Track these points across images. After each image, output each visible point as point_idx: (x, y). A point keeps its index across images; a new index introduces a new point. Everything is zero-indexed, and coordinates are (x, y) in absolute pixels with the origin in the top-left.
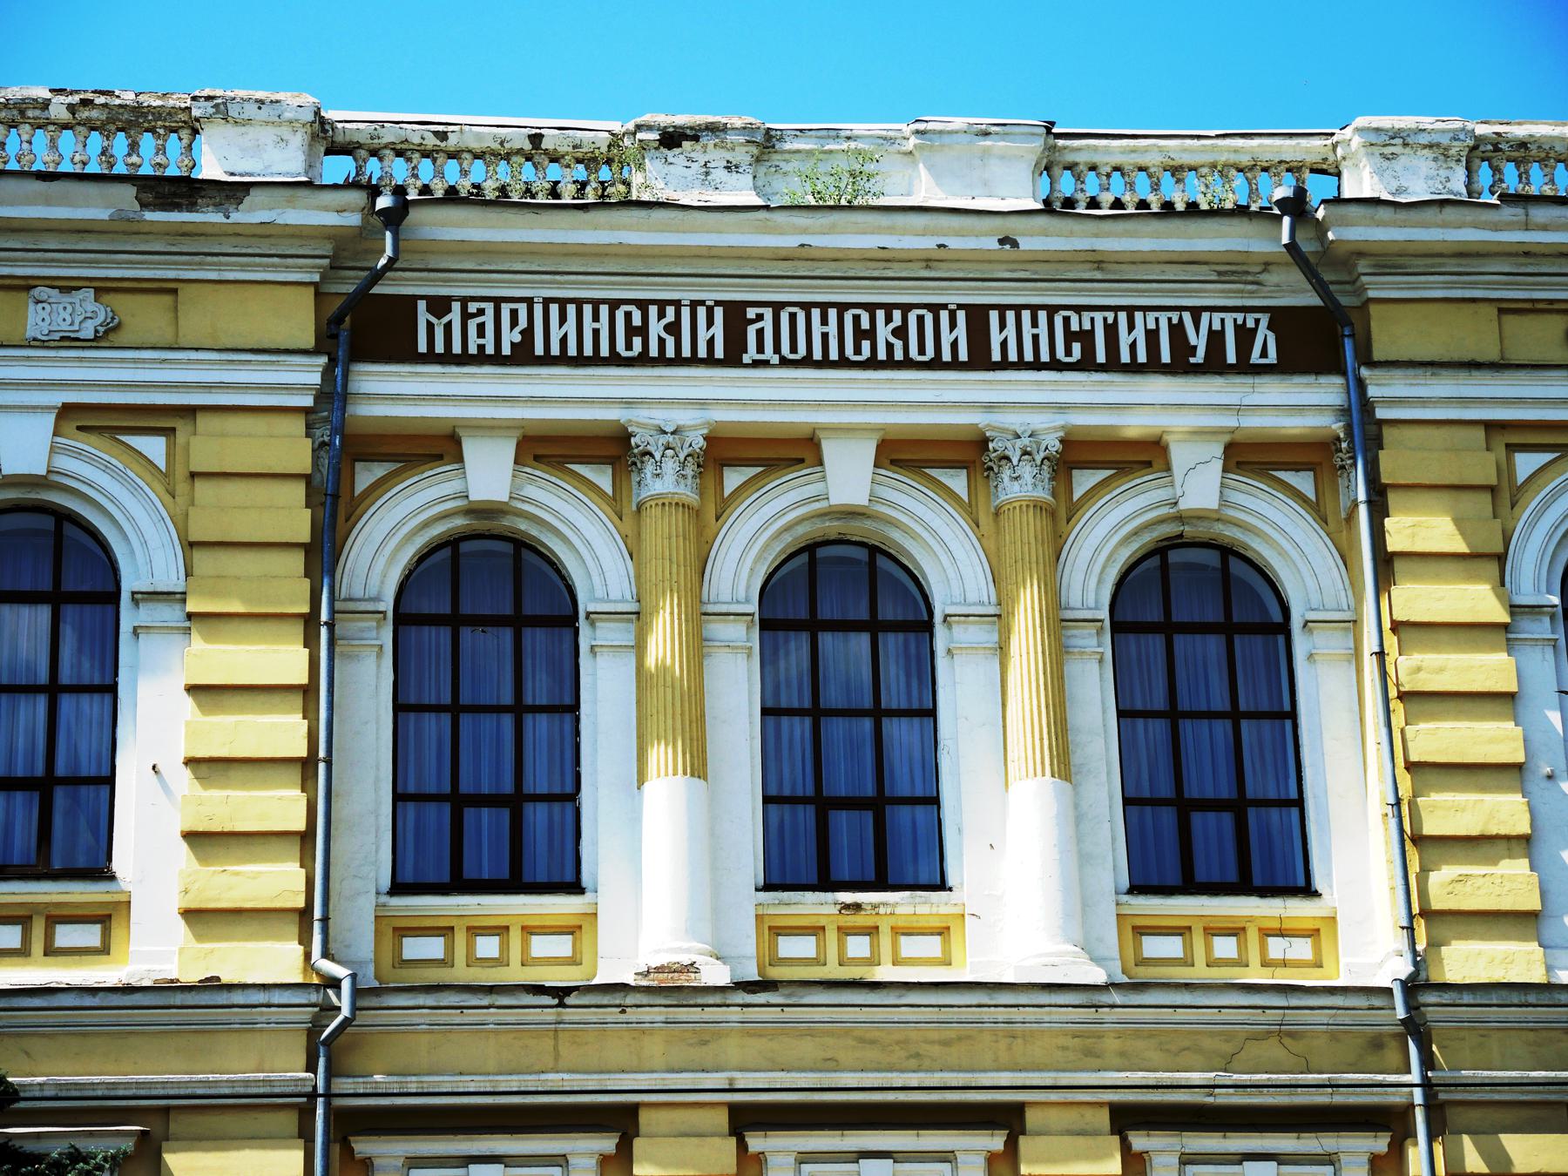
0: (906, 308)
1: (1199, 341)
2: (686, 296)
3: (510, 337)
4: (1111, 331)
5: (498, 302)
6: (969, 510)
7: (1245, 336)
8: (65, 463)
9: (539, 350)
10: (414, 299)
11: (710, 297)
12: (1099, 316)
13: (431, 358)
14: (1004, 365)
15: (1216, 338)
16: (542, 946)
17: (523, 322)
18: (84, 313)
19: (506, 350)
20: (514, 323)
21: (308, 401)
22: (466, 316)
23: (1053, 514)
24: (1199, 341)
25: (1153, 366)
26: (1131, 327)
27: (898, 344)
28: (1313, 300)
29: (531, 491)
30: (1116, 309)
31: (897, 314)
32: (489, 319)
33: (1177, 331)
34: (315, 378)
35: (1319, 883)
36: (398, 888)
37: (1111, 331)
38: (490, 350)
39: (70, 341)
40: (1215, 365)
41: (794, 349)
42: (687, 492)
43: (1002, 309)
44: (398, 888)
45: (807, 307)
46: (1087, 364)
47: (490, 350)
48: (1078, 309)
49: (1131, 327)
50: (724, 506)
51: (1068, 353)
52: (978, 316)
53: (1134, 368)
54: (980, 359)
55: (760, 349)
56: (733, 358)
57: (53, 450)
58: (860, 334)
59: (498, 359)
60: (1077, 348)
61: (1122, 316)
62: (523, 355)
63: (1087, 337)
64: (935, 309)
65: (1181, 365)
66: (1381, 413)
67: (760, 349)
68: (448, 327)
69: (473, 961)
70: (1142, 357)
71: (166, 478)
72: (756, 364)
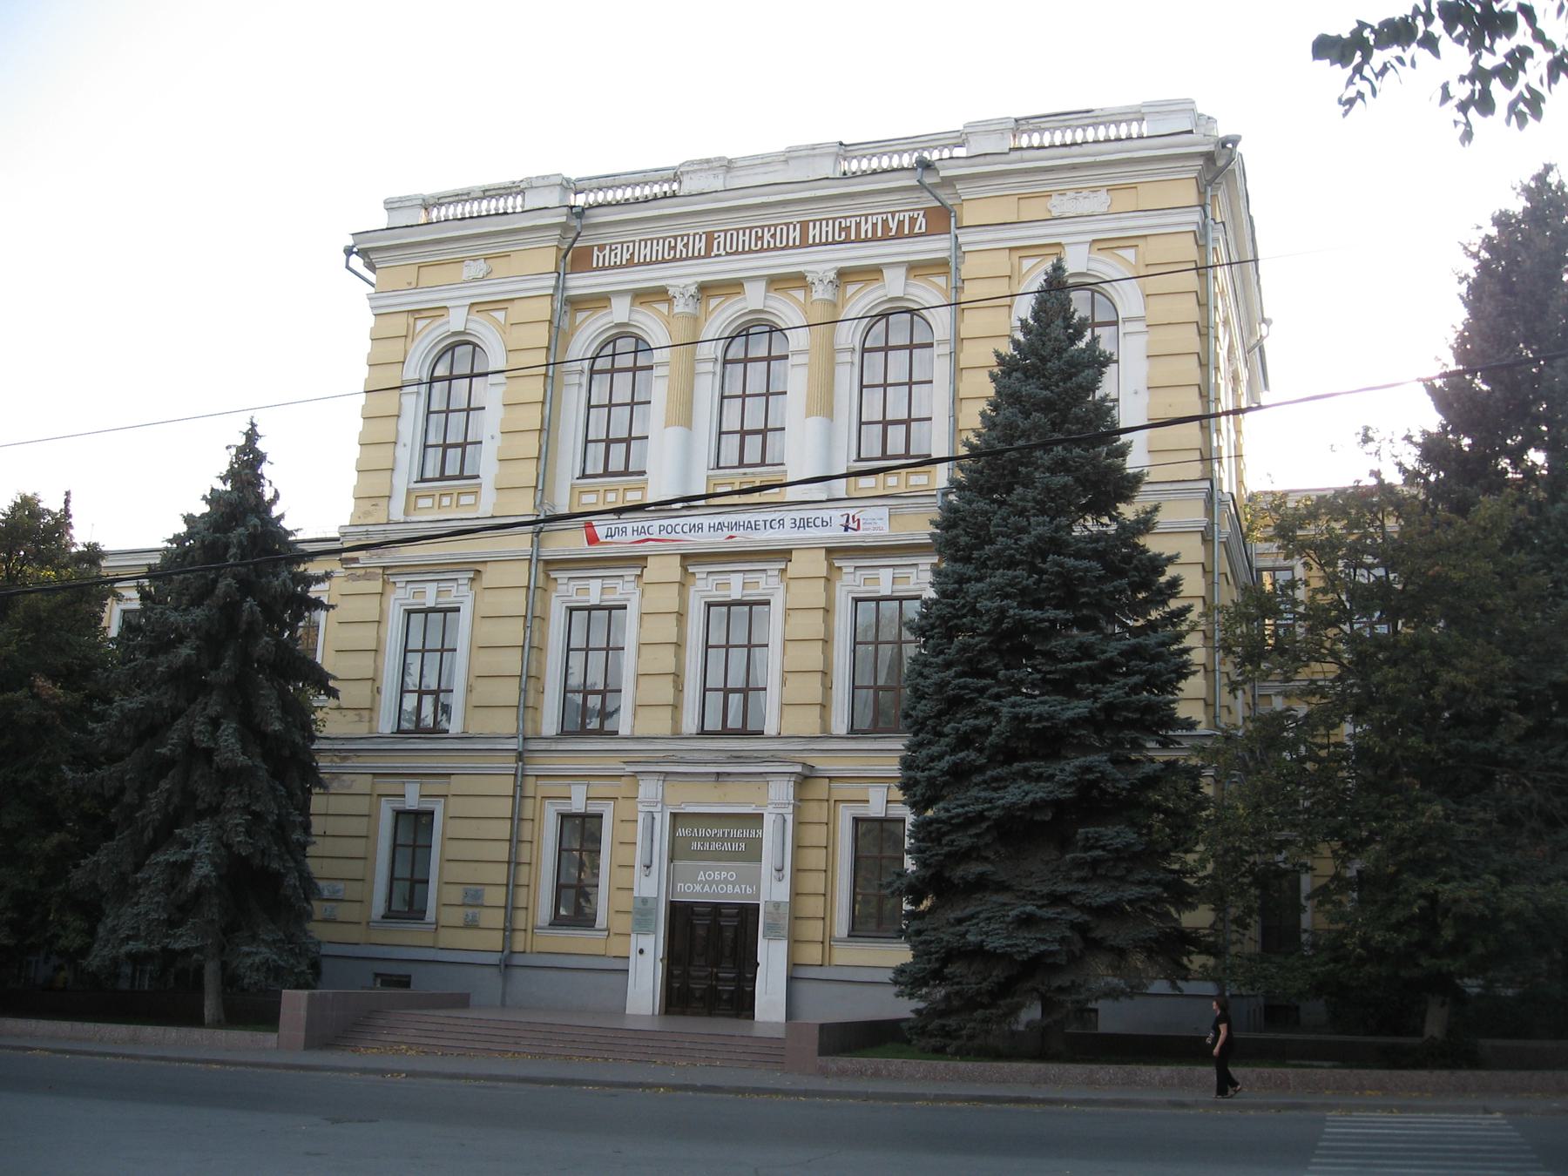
0: (776, 226)
1: (893, 225)
3: (626, 256)
4: (858, 225)
5: (622, 243)
7: (913, 220)
9: (636, 261)
10: (593, 246)
12: (853, 220)
13: (598, 269)
15: (900, 223)
17: (631, 250)
19: (624, 262)
21: (551, 292)
22: (611, 250)
24: (893, 225)
25: (874, 239)
26: (866, 223)
28: (939, 204)
30: (860, 216)
31: (773, 229)
32: (619, 251)
33: (885, 222)
37: (858, 225)
39: (475, 279)
40: (899, 236)
41: (731, 248)
44: (584, 476)
45: (737, 230)
46: (847, 241)
47: (618, 263)
48: (845, 218)
49: (866, 223)
50: (707, 314)
51: (840, 236)
52: (804, 226)
53: (866, 240)
54: (804, 244)
55: (718, 249)
56: (707, 255)
58: (757, 238)
59: (621, 266)
60: (843, 234)
61: (890, 216)
62: (630, 263)
66: (964, 249)
67: (718, 249)
68: (604, 256)
70: (870, 235)
72: (716, 256)
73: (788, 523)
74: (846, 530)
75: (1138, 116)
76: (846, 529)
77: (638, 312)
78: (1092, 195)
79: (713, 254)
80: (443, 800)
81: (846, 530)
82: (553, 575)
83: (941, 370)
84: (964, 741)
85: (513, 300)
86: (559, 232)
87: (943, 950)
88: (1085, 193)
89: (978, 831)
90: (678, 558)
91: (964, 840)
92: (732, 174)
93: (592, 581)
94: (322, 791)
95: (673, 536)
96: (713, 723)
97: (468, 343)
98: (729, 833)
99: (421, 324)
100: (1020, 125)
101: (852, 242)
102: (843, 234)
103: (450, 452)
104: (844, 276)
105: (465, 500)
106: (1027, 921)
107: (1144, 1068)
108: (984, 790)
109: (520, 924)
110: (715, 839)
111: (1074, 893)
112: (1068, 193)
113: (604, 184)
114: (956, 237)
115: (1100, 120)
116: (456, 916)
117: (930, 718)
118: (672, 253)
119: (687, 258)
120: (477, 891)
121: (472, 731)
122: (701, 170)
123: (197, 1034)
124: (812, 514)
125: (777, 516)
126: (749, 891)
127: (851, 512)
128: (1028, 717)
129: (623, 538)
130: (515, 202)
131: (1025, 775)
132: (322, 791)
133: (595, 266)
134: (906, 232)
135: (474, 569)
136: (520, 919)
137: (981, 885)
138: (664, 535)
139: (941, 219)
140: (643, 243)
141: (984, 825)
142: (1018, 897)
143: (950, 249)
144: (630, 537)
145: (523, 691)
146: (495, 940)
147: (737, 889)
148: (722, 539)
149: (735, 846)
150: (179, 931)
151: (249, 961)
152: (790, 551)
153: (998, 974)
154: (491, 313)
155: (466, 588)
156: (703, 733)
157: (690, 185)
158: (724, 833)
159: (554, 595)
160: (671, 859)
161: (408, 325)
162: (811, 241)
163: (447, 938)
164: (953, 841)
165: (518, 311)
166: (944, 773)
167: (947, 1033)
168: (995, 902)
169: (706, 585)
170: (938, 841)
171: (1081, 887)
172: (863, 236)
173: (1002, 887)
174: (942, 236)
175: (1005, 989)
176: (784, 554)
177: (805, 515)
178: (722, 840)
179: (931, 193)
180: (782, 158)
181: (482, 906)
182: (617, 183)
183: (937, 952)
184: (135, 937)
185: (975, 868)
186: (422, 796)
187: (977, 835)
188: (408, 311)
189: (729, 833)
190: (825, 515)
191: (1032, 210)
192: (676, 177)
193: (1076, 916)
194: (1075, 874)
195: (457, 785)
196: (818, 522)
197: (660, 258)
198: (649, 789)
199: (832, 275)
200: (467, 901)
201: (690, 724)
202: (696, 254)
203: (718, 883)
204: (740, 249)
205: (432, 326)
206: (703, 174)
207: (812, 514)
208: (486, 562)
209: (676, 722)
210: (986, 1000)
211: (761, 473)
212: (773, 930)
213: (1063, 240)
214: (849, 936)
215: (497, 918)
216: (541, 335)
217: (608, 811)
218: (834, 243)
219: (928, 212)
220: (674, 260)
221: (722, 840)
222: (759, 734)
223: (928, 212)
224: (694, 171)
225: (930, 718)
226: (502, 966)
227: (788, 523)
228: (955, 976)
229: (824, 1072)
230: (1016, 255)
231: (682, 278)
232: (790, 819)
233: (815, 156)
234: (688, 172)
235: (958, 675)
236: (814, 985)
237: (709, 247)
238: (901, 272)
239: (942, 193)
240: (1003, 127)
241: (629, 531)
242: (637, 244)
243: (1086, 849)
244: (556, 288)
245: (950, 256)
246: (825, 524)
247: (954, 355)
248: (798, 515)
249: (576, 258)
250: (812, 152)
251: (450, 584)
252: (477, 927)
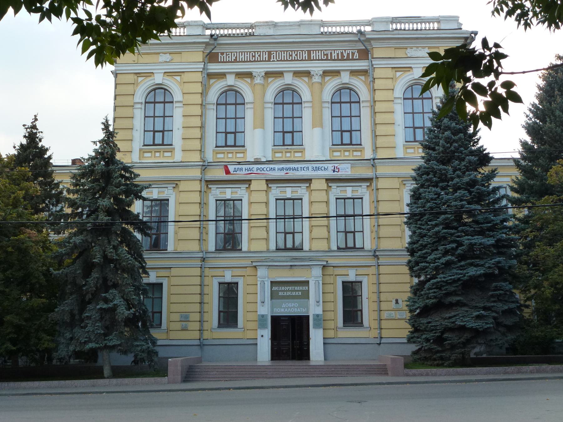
0: (297, 51)
1: (345, 55)
2: (262, 50)
3: (233, 58)
4: (331, 53)
5: (231, 52)
6: (308, 84)
7: (353, 54)
8: (165, 81)
9: (238, 60)
10: (218, 53)
11: (265, 50)
12: (329, 51)
13: (221, 62)
14: (313, 60)
15: (348, 54)
16: (238, 155)
17: (235, 56)
18: (167, 57)
19: (233, 60)
20: (234, 56)
21: (201, 70)
22: (227, 55)
23: (321, 84)
24: (345, 55)
25: (338, 60)
26: (334, 53)
27: (259, 58)
28: (364, 48)
29: (238, 83)
31: (296, 52)
32: (230, 55)
33: (342, 53)
34: (202, 66)
35: (362, 144)
36: (216, 147)
37: (331, 53)
38: (230, 60)
39: (166, 62)
40: (348, 59)
41: (279, 58)
42: (262, 82)
43: (313, 50)
44: (216, 147)
45: (281, 51)
46: (327, 59)
47: (230, 60)
48: (326, 50)
49: (334, 53)
50: (268, 84)
51: (324, 57)
52: (309, 52)
53: (334, 60)
54: (309, 59)
55: (274, 59)
56: (269, 61)
57: (163, 79)
58: (290, 55)
59: (231, 62)
60: (325, 57)
62: (235, 61)
63: (327, 55)
64: (302, 51)
65: (343, 59)
66: (374, 66)
67: (274, 59)
68: (224, 57)
69: (228, 158)
70: (336, 58)
72: (273, 61)
73: (310, 168)
74: (334, 172)
75: (437, 20)
76: (334, 172)
77: (238, 81)
78: (422, 49)
79: (271, 60)
80: (367, 276)
81: (334, 172)
82: (210, 186)
83: (366, 113)
84: (446, 253)
85: (184, 72)
86: (204, 45)
87: (443, 328)
88: (420, 48)
89: (458, 285)
90: (265, 181)
91: (451, 288)
92: (277, 28)
94: (146, 276)
95: (263, 172)
96: (281, 245)
97: (162, 88)
98: (294, 288)
99: (140, 79)
100: (395, 20)
101: (329, 60)
102: (325, 57)
103: (229, 135)
104: (326, 73)
105: (166, 154)
106: (478, 317)
107: (524, 367)
108: (457, 270)
109: (205, 328)
110: (289, 291)
111: (493, 306)
112: (414, 48)
113: (220, 27)
114: (371, 61)
115: (423, 21)
116: (178, 326)
117: (430, 244)
118: (254, 58)
119: (260, 61)
120: (186, 315)
121: (179, 250)
122: (264, 25)
123: (100, 381)
124: (321, 165)
125: (306, 166)
126: (304, 310)
127: (336, 165)
128: (475, 244)
129: (241, 172)
130: (180, 30)
131: (472, 264)
132: (146, 276)
133: (220, 61)
134: (351, 58)
135: (175, 183)
136: (206, 326)
137: (459, 304)
138: (259, 172)
139: (365, 54)
140: (240, 53)
141: (460, 283)
142: (470, 308)
143: (369, 66)
144: (244, 172)
145: (201, 233)
146: (196, 335)
147: (299, 310)
148: (283, 174)
149: (297, 293)
150: (111, 337)
151: (139, 348)
152: (311, 180)
153: (467, 335)
154: (174, 77)
155: (172, 191)
156: (278, 249)
157: (257, 31)
158: (292, 288)
159: (210, 194)
160: (271, 299)
161: (135, 79)
162: (312, 59)
163: (172, 335)
164: (447, 289)
165: (186, 77)
166: (442, 264)
167: (441, 358)
168: (463, 310)
169: (276, 191)
170: (440, 289)
171: (495, 304)
172: (333, 58)
173: (464, 305)
174: (365, 61)
175: (468, 342)
176: (309, 181)
177: (317, 165)
178: (292, 291)
179: (363, 44)
180: (298, 24)
181: (189, 321)
182: (225, 27)
183: (440, 329)
184: (90, 341)
185: (455, 299)
186: (157, 277)
187: (457, 286)
188: (134, 73)
189: (294, 288)
190: (326, 166)
191: (400, 54)
192: (252, 26)
193: (494, 314)
194: (492, 299)
195: (174, 272)
196: (323, 168)
197: (248, 60)
198: (262, 272)
199: (321, 73)
200: (182, 320)
201: (273, 247)
202: (264, 60)
203: (291, 308)
204: (283, 59)
205: (146, 81)
206: (264, 27)
207: (321, 165)
208: (180, 180)
209: (268, 244)
210: (462, 346)
211: (294, 149)
212: (316, 326)
214: (344, 326)
215: (197, 326)
216: (198, 88)
217: (365, 280)
218: (322, 60)
219: (359, 51)
220: (255, 61)
221: (292, 291)
222: (301, 249)
223: (359, 51)
224: (261, 26)
225: (430, 244)
226: (202, 345)
227: (310, 168)
228: (449, 338)
229: (407, 375)
230: (394, 70)
231: (258, 69)
232: (321, 282)
233: (311, 24)
234: (258, 26)
235: (443, 228)
236: (332, 345)
237: (270, 58)
238: (348, 73)
239: (366, 44)
240: (387, 20)
241: (244, 169)
242: (238, 53)
243: (495, 290)
244: (204, 69)
245: (369, 69)
246: (325, 169)
247: (373, 107)
248: (314, 166)
249: (212, 57)
250: (310, 23)
251: (237, 189)
252: (187, 330)
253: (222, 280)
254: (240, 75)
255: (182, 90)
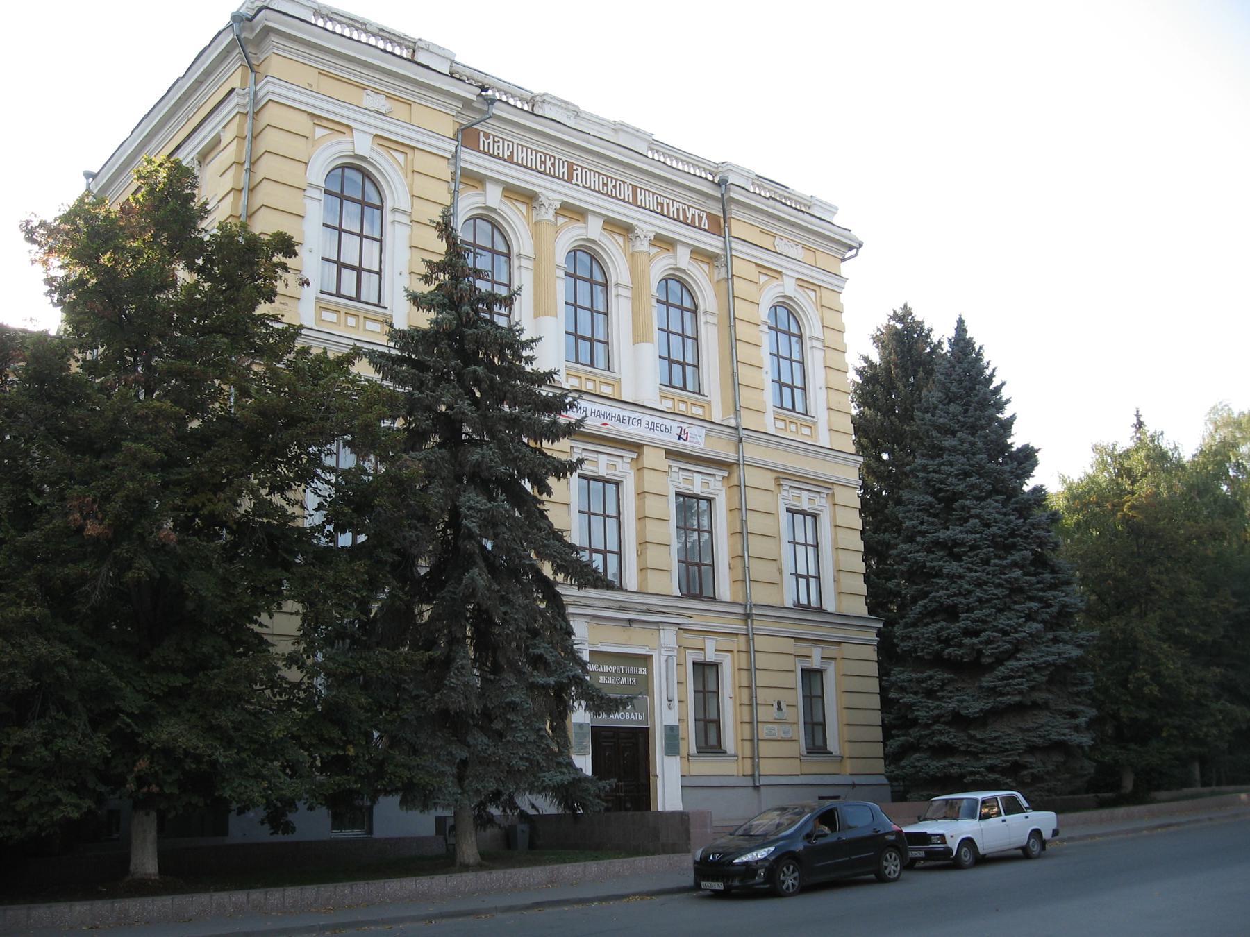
3: (507, 153)
17: (511, 150)
18: (381, 103)
20: (508, 149)
22: (494, 142)
30: (670, 199)
33: (684, 210)
37: (668, 204)
38: (501, 156)
48: (660, 195)
55: (577, 180)
59: (502, 159)
60: (659, 207)
62: (510, 160)
66: (733, 253)
67: (577, 180)
68: (489, 143)
71: (404, 170)
74: (679, 439)
76: (680, 438)
81: (679, 439)
85: (413, 148)
92: (578, 121)
93: (600, 456)
127: (684, 426)
139: (718, 225)
148: (599, 424)
174: (713, 236)
177: (656, 420)
180: (613, 127)
188: (309, 113)
190: (668, 423)
191: (766, 242)
207: (660, 421)
213: (784, 271)
224: (554, 105)
231: (553, 192)
233: (637, 137)
234: (549, 103)
246: (667, 431)
249: (467, 136)
253: (700, 657)
254: (512, 192)
255: (411, 187)
